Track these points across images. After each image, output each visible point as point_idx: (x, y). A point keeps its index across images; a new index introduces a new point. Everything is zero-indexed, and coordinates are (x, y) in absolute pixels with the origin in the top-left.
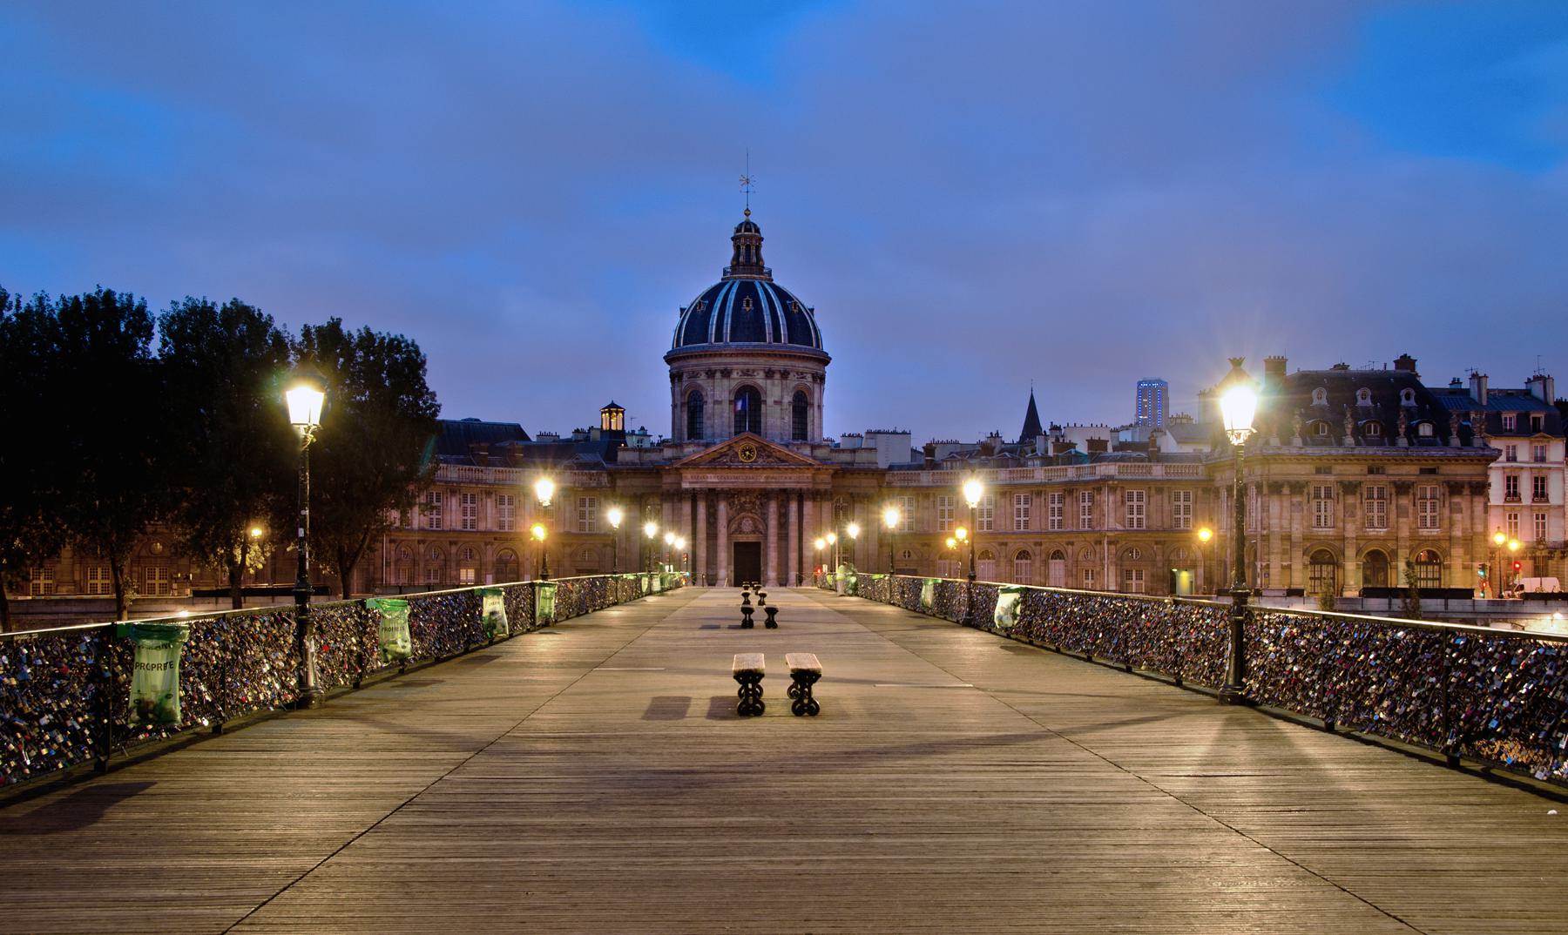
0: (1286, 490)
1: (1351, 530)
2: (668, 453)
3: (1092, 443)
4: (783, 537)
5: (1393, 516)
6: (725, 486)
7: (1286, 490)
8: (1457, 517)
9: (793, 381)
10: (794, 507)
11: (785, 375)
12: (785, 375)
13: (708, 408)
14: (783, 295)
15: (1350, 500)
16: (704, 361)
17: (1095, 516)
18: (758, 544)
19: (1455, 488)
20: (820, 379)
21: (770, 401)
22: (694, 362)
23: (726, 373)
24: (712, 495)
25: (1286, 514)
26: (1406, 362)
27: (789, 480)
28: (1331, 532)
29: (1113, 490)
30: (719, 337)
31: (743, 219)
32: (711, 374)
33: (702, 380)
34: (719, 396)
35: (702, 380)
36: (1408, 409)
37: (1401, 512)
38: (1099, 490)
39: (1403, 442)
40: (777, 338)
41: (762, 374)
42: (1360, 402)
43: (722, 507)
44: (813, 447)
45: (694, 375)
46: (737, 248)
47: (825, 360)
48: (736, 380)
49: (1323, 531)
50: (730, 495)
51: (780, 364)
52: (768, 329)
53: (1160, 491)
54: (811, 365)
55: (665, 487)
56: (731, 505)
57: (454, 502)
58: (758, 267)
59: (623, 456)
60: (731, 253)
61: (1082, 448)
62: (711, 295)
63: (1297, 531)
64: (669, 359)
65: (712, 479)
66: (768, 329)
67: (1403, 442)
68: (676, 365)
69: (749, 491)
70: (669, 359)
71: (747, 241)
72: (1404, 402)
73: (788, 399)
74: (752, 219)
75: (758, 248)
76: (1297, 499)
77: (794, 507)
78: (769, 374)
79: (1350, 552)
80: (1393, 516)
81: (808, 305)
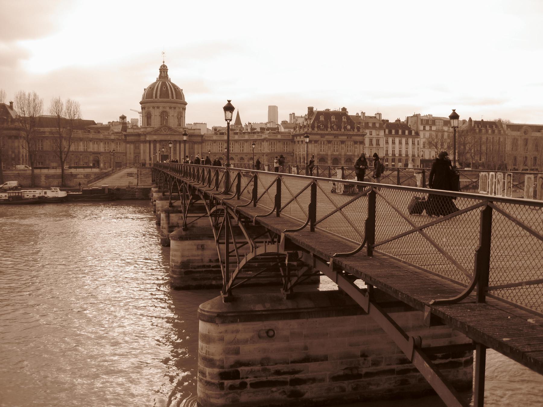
0: (313, 142)
1: (329, 153)
2: (142, 130)
3: (261, 128)
4: (175, 153)
5: (340, 149)
6: (159, 139)
7: (313, 142)
8: (356, 150)
9: (177, 110)
10: (178, 145)
11: (175, 108)
12: (175, 108)
13: (153, 117)
14: (174, 86)
15: (329, 145)
16: (152, 104)
17: (262, 148)
18: (168, 155)
19: (356, 143)
20: (185, 109)
21: (171, 115)
22: (149, 104)
23: (158, 107)
24: (155, 142)
25: (313, 148)
26: (344, 109)
27: (177, 138)
28: (324, 153)
29: (267, 141)
30: (156, 97)
31: (162, 64)
32: (154, 108)
33: (151, 109)
34: (156, 114)
35: (151, 109)
36: (344, 122)
37: (342, 148)
38: (263, 141)
39: (343, 130)
40: (173, 98)
41: (168, 108)
42: (332, 120)
43: (158, 145)
44: (184, 129)
45: (149, 108)
46: (161, 72)
47: (186, 104)
48: (161, 109)
49: (322, 153)
50: (161, 141)
51: (173, 105)
52: (170, 95)
53: (280, 142)
54: (183, 105)
55: (141, 139)
56: (160, 144)
57: (81, 143)
58: (167, 76)
59: (128, 131)
60: (159, 73)
61: (259, 130)
62: (154, 84)
63: (316, 154)
64: (141, 103)
65: (155, 137)
66: (170, 95)
67: (343, 130)
68: (143, 105)
69: (165, 141)
70: (141, 103)
71: (164, 70)
72: (343, 120)
73: (176, 115)
74: (165, 64)
75: (167, 72)
76: (316, 145)
77: (178, 145)
78: (170, 108)
79: (329, 159)
80: (340, 149)
81: (181, 88)
